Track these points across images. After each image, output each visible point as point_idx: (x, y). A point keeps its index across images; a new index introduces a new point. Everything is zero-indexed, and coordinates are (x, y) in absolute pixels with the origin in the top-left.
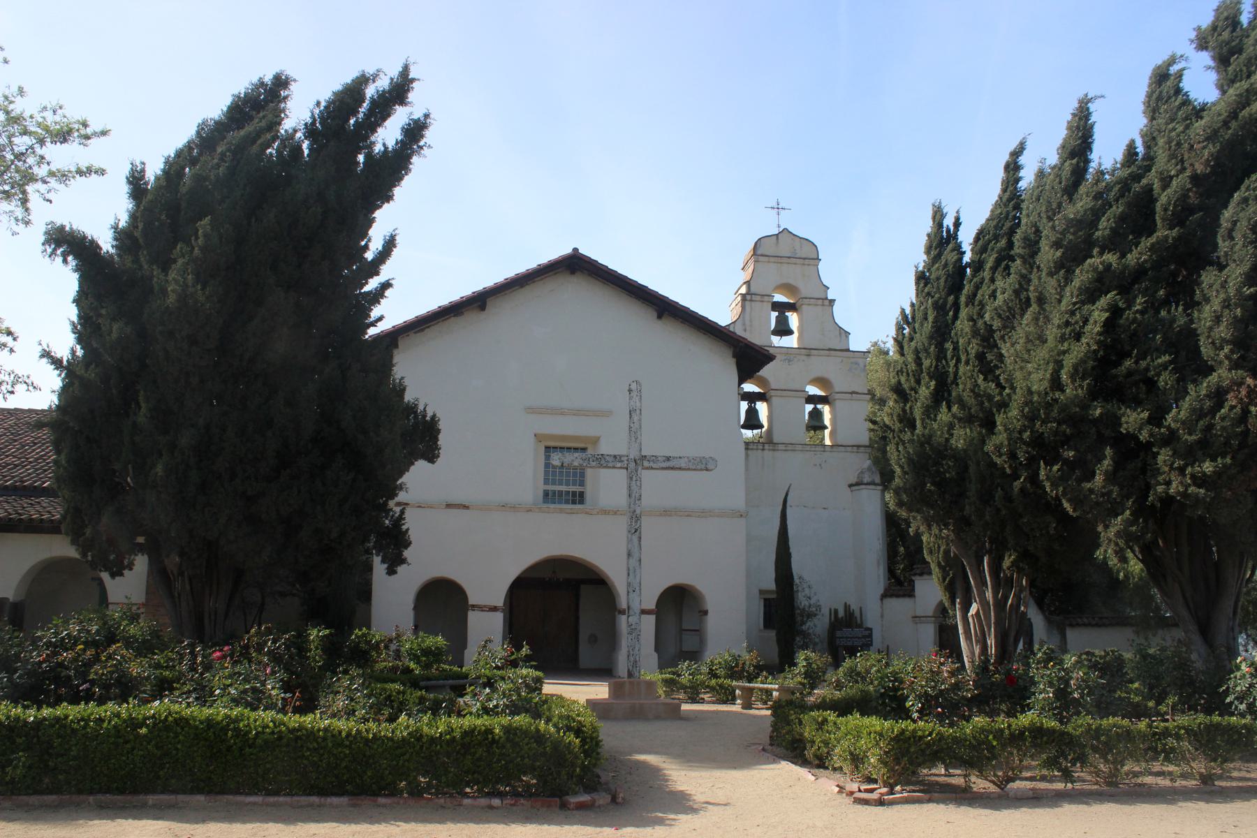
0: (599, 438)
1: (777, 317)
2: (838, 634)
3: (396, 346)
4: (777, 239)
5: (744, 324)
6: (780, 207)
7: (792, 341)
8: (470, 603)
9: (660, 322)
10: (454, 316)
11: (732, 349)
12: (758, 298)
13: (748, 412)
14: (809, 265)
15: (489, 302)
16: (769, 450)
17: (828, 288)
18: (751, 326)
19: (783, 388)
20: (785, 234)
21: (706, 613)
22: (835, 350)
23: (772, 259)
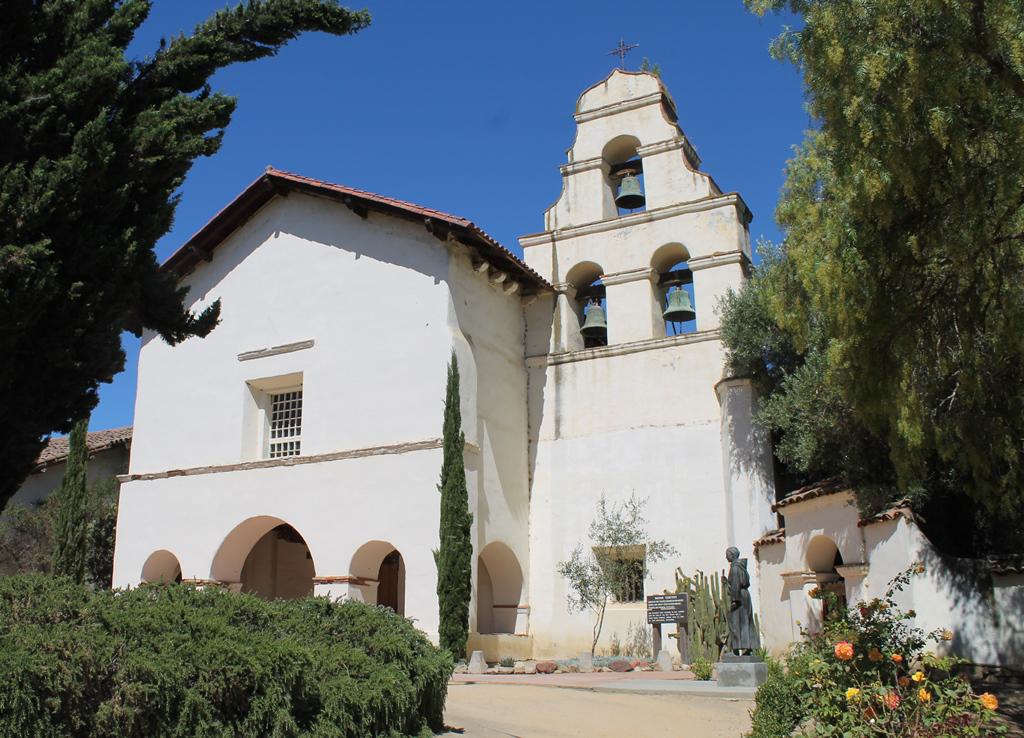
0: (302, 373)
5: (568, 203)
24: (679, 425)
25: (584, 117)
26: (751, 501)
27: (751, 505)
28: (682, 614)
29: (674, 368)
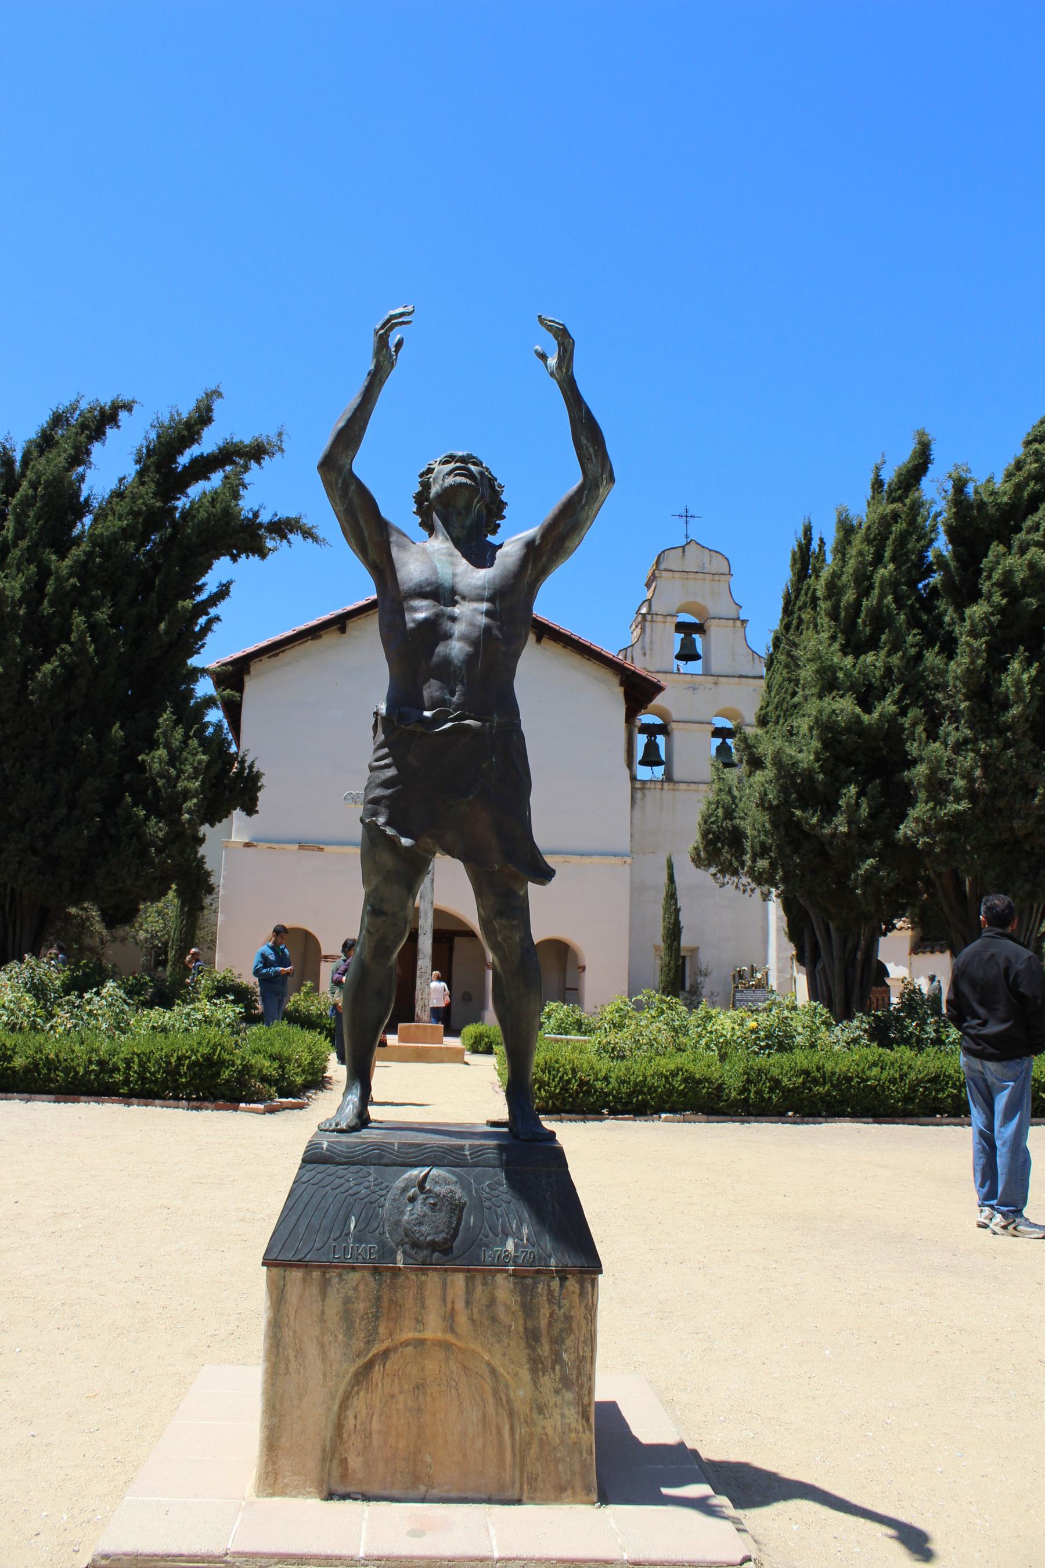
1: (682, 639)
3: (249, 673)
4: (684, 551)
5: (643, 648)
7: (695, 667)
8: (324, 953)
9: (539, 647)
10: (312, 639)
11: (619, 677)
12: (660, 618)
13: (647, 746)
15: (351, 624)
18: (651, 649)
19: (686, 719)
20: (693, 545)
21: (584, 968)
22: (747, 677)
23: (677, 575)
25: (664, 574)
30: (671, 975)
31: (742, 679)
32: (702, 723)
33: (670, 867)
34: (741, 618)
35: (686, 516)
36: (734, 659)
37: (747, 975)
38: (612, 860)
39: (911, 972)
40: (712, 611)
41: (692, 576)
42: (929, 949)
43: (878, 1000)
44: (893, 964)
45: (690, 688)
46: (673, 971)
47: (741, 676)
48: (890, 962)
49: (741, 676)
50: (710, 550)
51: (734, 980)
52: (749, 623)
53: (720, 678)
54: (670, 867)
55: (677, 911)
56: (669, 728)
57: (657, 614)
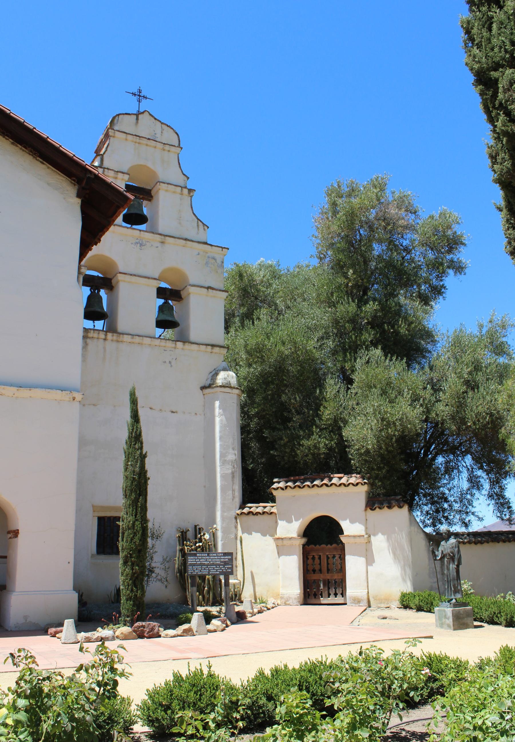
2: (191, 560)
4: (137, 119)
6: (141, 94)
11: (77, 187)
13: (89, 298)
14: (169, 151)
16: (112, 340)
17: (188, 178)
21: (16, 533)
23: (130, 137)
24: (172, 412)
25: (118, 134)
26: (233, 481)
27: (233, 483)
28: (228, 568)
29: (171, 366)
30: (137, 540)
31: (188, 242)
32: (149, 278)
33: (134, 402)
34: (189, 187)
35: (140, 96)
36: (180, 223)
37: (190, 535)
38: (58, 395)
39: (366, 528)
40: (162, 175)
41: (145, 141)
42: (385, 505)
43: (328, 558)
44: (348, 521)
45: (137, 243)
46: (139, 535)
47: (186, 239)
48: (345, 519)
49: (186, 239)
50: (162, 123)
51: (179, 541)
52: (195, 193)
53: (167, 238)
54: (134, 402)
55: (143, 457)
56: (114, 282)
57: (108, 169)
